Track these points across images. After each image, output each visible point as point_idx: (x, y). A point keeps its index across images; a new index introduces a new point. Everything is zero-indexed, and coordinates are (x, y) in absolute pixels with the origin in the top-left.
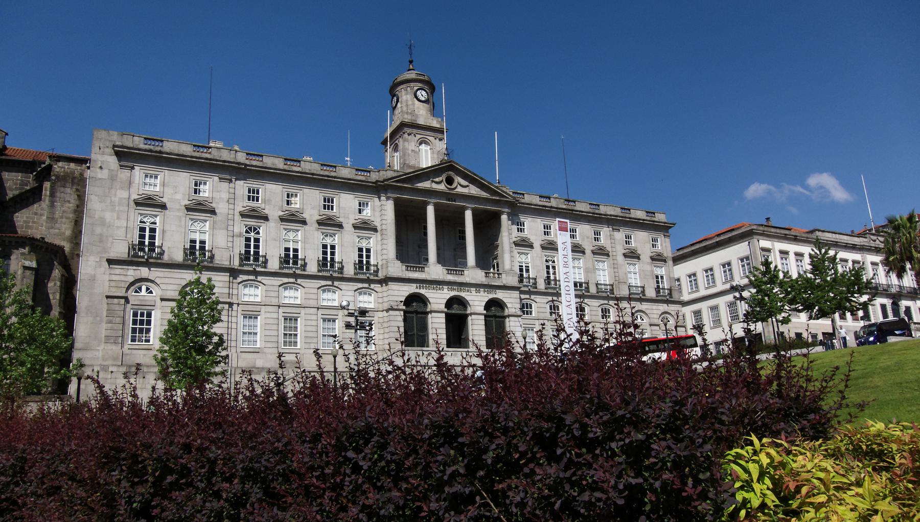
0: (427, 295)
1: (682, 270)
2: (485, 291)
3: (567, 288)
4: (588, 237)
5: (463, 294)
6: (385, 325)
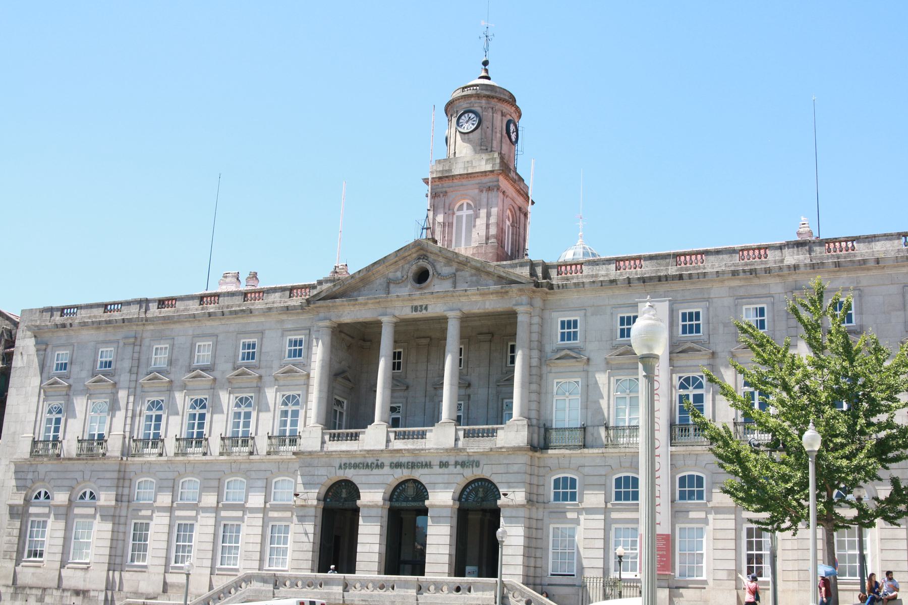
0: (355, 480)
2: (456, 463)
4: (726, 325)
5: (417, 474)
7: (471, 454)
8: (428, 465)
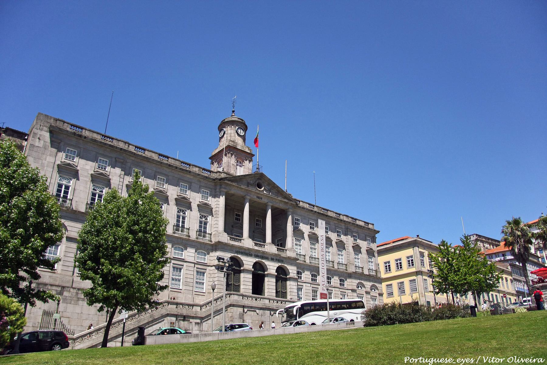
1: (382, 260)
2: (276, 260)
3: (323, 265)
6: (212, 276)
7: (281, 257)
8: (267, 258)
